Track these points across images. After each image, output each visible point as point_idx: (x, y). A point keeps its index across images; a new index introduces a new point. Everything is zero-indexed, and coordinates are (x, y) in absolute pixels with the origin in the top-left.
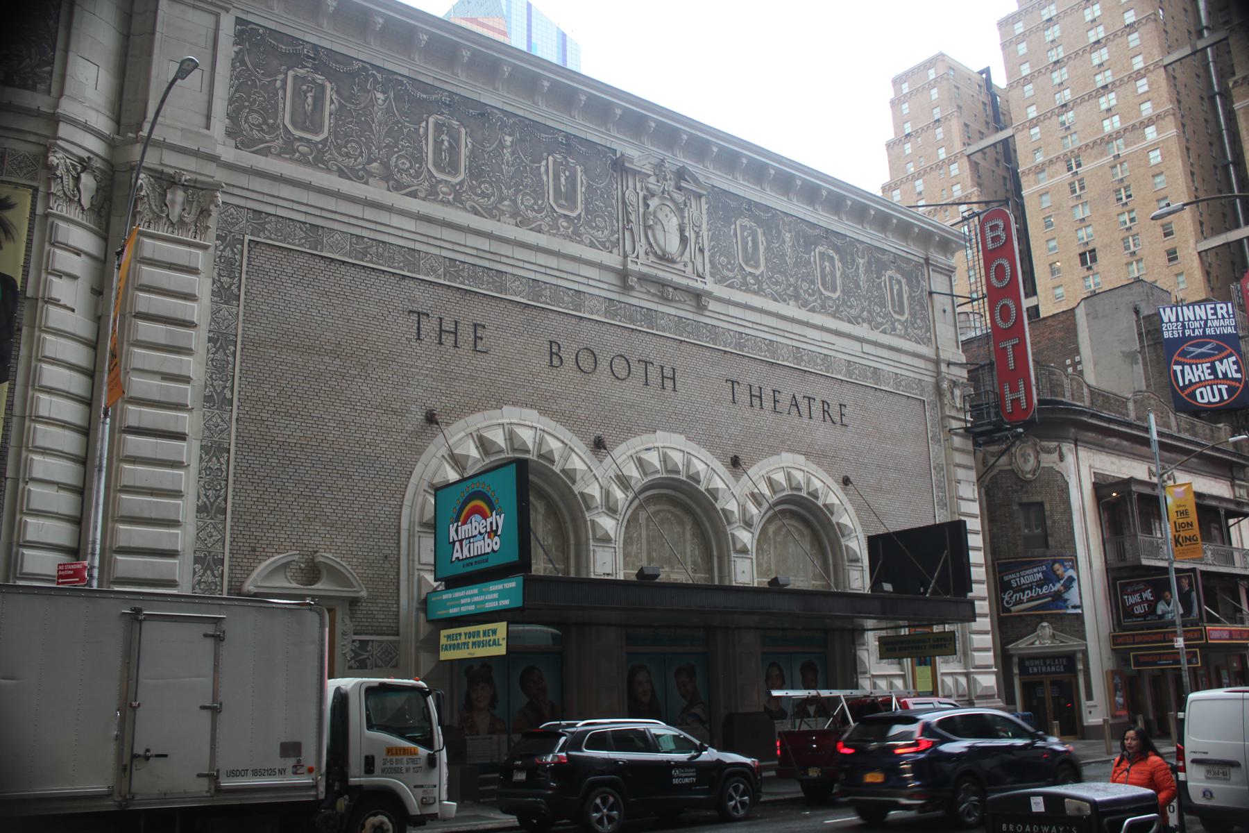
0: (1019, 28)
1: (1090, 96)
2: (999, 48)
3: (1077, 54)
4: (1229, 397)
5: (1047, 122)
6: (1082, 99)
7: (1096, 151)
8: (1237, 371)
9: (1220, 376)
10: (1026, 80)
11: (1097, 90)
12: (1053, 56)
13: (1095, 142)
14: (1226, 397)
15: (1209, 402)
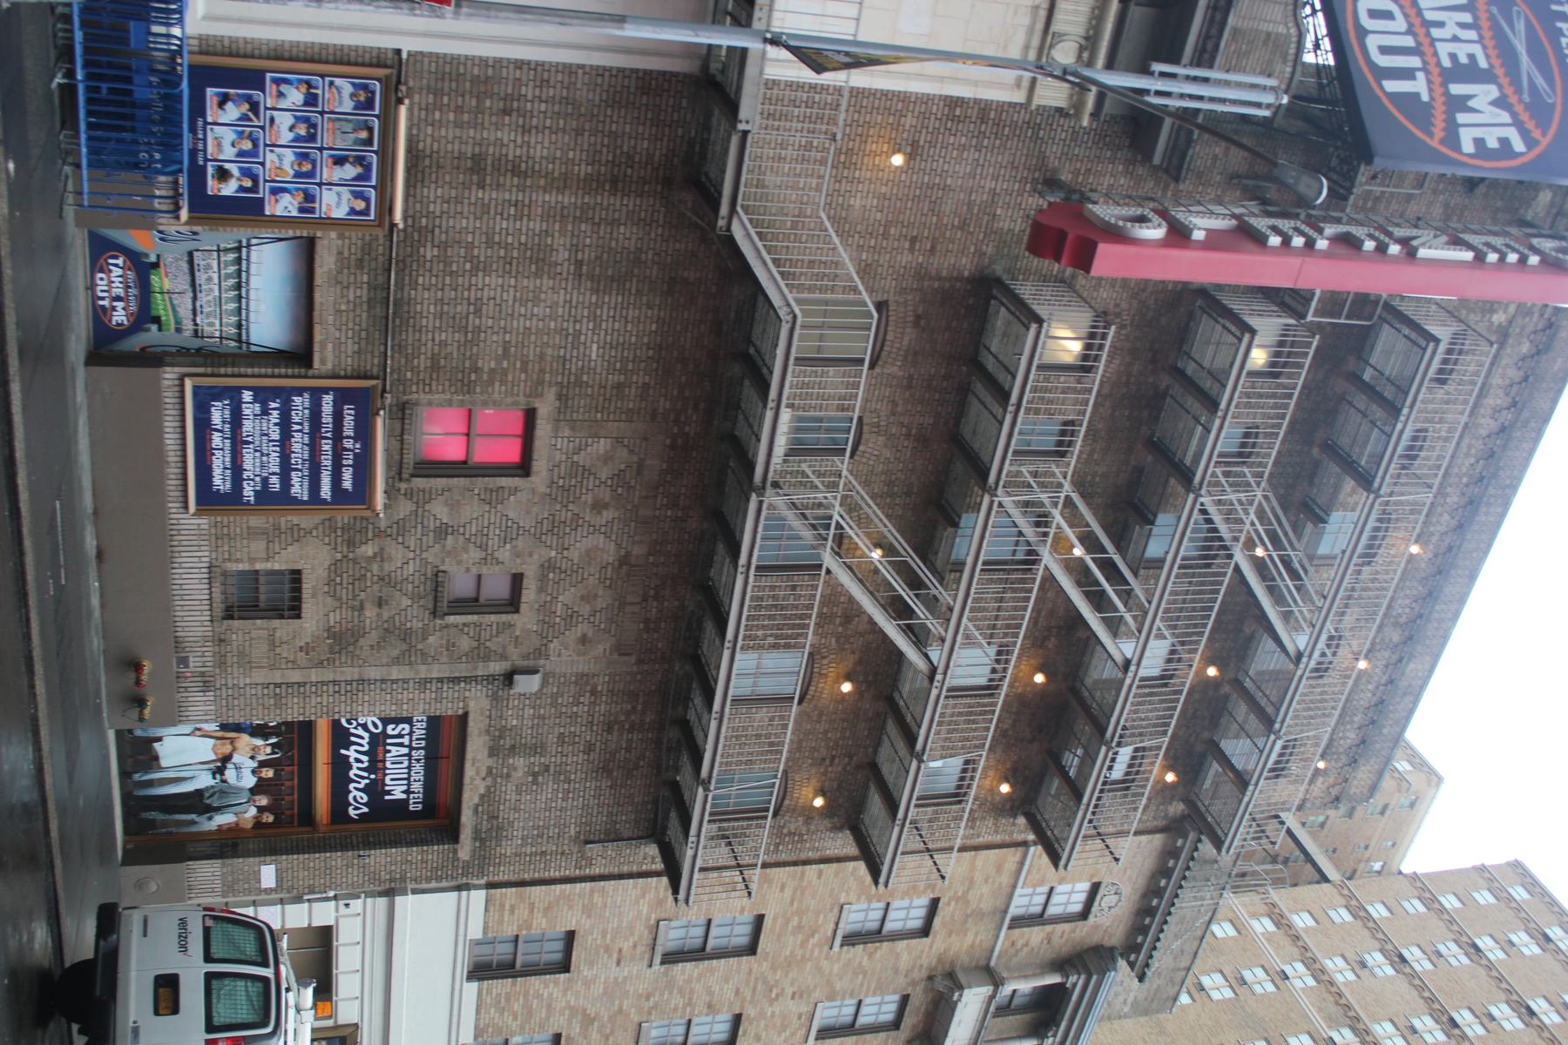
0: (1519, 893)
1: (1431, 1000)
2: (1478, 863)
3: (1500, 979)
4: (1396, 97)
5: (1366, 933)
6: (1422, 988)
7: (1333, 1009)
8: (1479, 142)
9: (1456, 89)
10: (1431, 902)
11: (1444, 1011)
12: (1485, 943)
13: (1348, 1007)
14: (1391, 86)
15: (1363, 33)
